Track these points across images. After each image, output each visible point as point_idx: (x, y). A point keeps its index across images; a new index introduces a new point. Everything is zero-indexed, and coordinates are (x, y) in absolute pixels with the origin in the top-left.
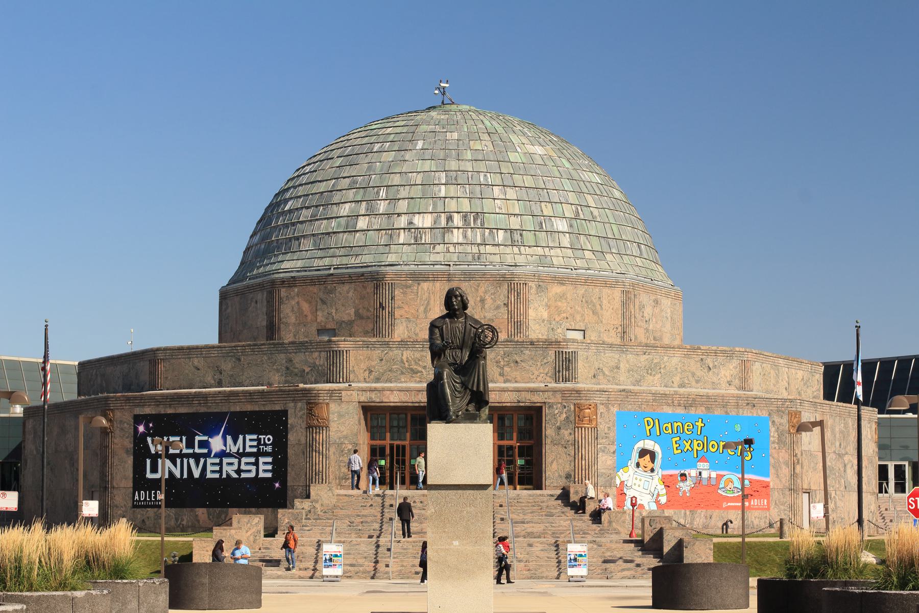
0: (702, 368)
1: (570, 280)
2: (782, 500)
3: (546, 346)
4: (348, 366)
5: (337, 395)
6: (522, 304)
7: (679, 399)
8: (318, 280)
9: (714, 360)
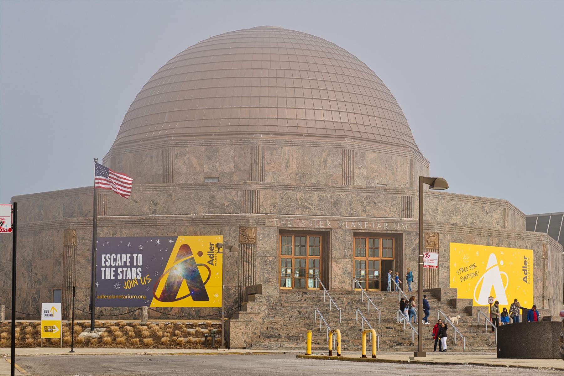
1: (379, 150)
3: (394, 192)
4: (259, 202)
5: (262, 221)
6: (351, 164)
7: (484, 232)
8: (205, 143)
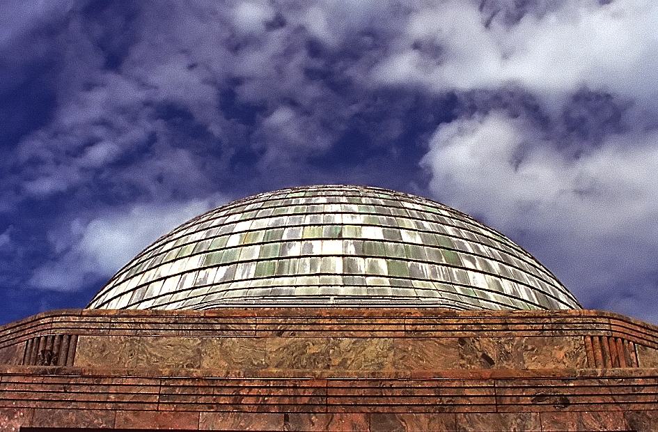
0: (463, 362)
7: (263, 392)
9: (503, 340)
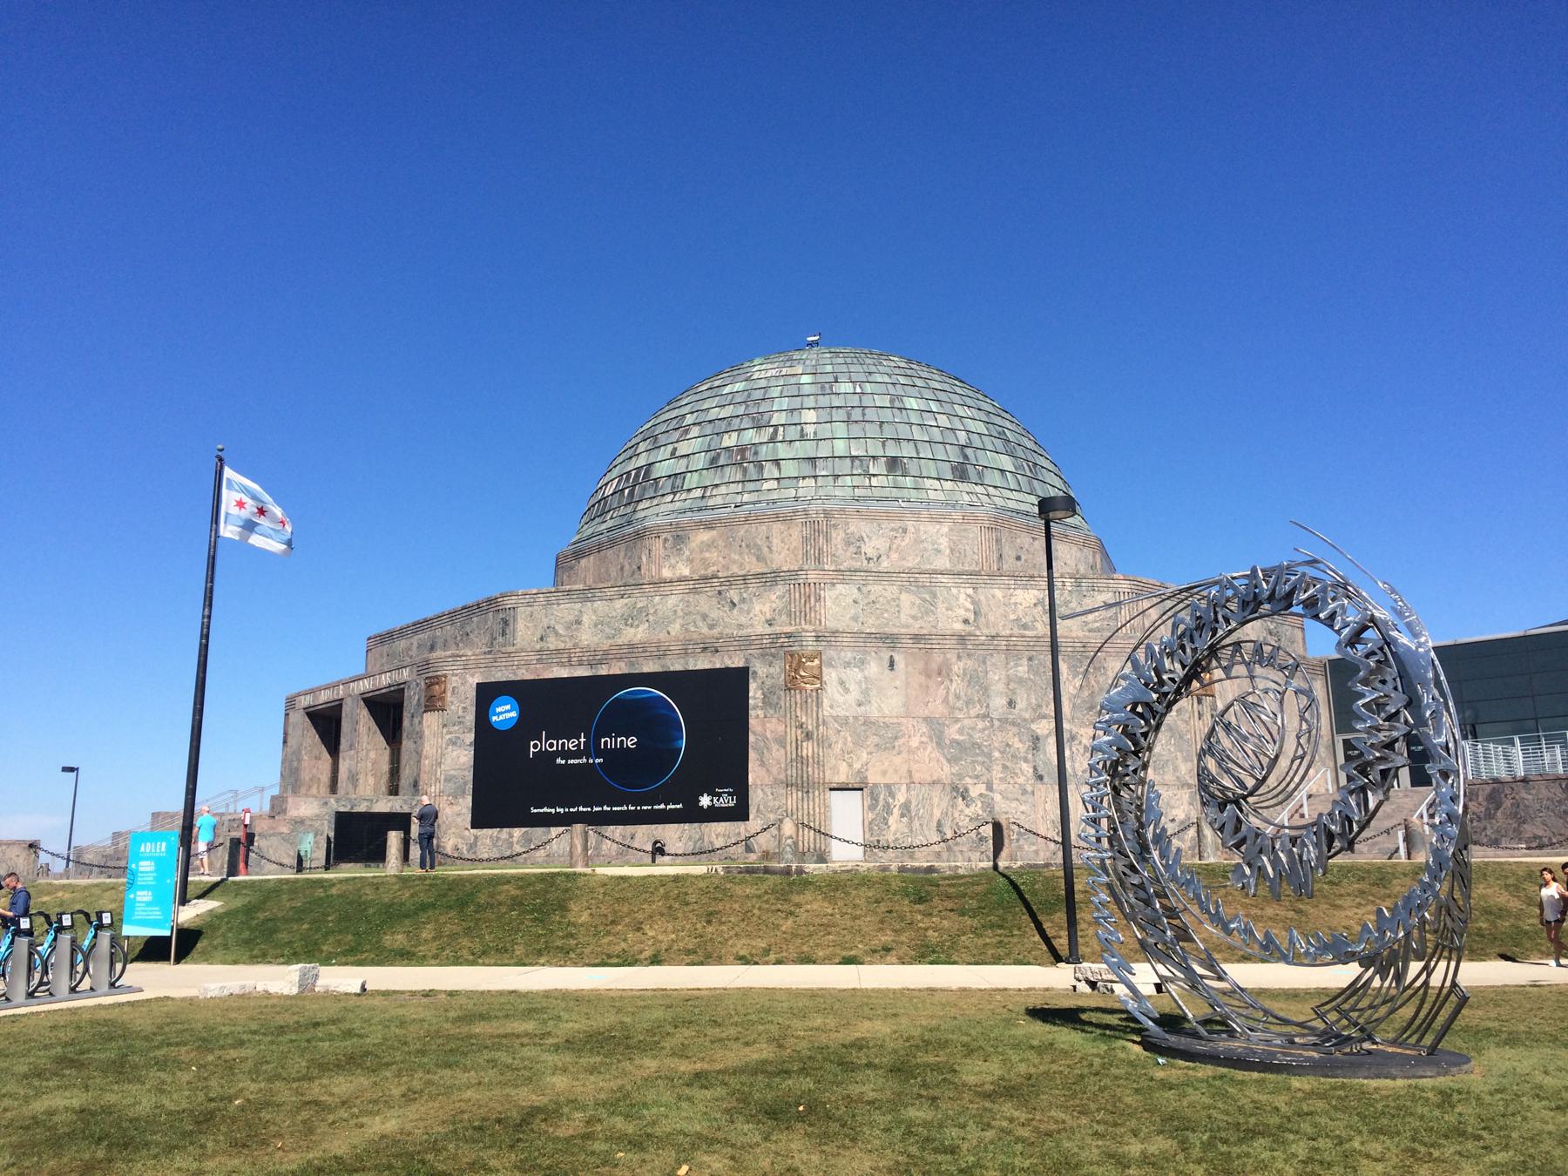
2: (771, 804)
7: (581, 654)
